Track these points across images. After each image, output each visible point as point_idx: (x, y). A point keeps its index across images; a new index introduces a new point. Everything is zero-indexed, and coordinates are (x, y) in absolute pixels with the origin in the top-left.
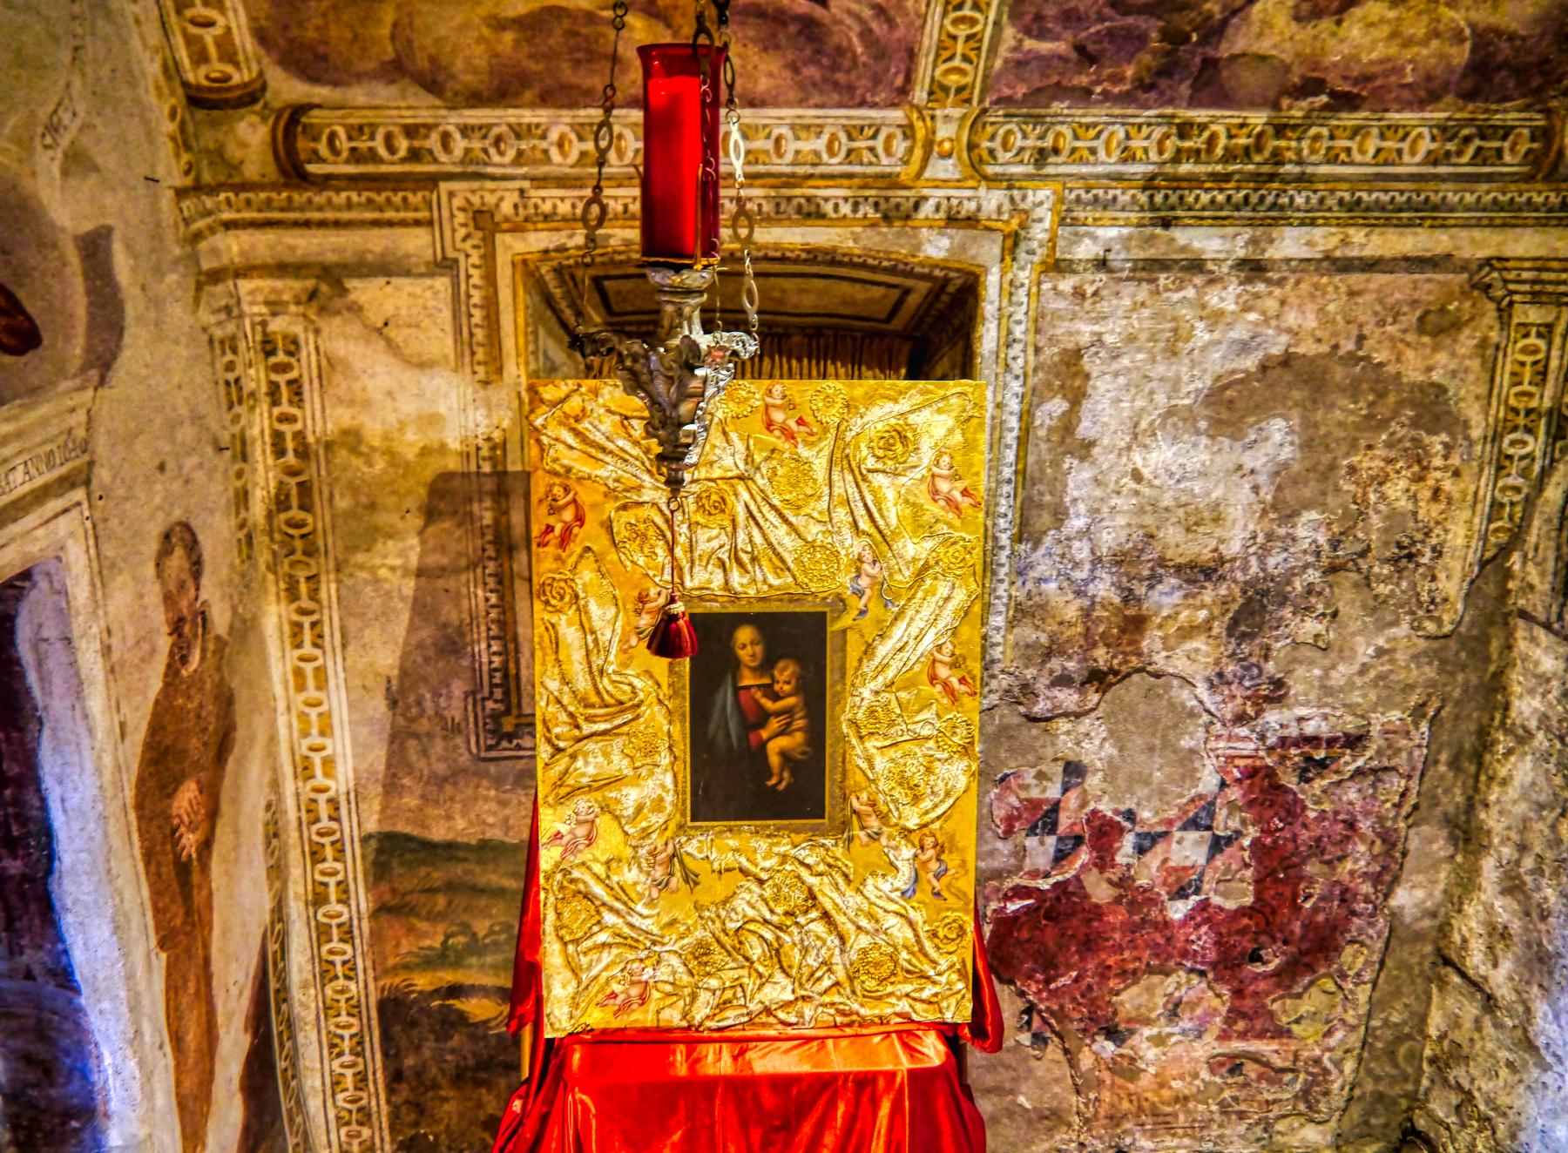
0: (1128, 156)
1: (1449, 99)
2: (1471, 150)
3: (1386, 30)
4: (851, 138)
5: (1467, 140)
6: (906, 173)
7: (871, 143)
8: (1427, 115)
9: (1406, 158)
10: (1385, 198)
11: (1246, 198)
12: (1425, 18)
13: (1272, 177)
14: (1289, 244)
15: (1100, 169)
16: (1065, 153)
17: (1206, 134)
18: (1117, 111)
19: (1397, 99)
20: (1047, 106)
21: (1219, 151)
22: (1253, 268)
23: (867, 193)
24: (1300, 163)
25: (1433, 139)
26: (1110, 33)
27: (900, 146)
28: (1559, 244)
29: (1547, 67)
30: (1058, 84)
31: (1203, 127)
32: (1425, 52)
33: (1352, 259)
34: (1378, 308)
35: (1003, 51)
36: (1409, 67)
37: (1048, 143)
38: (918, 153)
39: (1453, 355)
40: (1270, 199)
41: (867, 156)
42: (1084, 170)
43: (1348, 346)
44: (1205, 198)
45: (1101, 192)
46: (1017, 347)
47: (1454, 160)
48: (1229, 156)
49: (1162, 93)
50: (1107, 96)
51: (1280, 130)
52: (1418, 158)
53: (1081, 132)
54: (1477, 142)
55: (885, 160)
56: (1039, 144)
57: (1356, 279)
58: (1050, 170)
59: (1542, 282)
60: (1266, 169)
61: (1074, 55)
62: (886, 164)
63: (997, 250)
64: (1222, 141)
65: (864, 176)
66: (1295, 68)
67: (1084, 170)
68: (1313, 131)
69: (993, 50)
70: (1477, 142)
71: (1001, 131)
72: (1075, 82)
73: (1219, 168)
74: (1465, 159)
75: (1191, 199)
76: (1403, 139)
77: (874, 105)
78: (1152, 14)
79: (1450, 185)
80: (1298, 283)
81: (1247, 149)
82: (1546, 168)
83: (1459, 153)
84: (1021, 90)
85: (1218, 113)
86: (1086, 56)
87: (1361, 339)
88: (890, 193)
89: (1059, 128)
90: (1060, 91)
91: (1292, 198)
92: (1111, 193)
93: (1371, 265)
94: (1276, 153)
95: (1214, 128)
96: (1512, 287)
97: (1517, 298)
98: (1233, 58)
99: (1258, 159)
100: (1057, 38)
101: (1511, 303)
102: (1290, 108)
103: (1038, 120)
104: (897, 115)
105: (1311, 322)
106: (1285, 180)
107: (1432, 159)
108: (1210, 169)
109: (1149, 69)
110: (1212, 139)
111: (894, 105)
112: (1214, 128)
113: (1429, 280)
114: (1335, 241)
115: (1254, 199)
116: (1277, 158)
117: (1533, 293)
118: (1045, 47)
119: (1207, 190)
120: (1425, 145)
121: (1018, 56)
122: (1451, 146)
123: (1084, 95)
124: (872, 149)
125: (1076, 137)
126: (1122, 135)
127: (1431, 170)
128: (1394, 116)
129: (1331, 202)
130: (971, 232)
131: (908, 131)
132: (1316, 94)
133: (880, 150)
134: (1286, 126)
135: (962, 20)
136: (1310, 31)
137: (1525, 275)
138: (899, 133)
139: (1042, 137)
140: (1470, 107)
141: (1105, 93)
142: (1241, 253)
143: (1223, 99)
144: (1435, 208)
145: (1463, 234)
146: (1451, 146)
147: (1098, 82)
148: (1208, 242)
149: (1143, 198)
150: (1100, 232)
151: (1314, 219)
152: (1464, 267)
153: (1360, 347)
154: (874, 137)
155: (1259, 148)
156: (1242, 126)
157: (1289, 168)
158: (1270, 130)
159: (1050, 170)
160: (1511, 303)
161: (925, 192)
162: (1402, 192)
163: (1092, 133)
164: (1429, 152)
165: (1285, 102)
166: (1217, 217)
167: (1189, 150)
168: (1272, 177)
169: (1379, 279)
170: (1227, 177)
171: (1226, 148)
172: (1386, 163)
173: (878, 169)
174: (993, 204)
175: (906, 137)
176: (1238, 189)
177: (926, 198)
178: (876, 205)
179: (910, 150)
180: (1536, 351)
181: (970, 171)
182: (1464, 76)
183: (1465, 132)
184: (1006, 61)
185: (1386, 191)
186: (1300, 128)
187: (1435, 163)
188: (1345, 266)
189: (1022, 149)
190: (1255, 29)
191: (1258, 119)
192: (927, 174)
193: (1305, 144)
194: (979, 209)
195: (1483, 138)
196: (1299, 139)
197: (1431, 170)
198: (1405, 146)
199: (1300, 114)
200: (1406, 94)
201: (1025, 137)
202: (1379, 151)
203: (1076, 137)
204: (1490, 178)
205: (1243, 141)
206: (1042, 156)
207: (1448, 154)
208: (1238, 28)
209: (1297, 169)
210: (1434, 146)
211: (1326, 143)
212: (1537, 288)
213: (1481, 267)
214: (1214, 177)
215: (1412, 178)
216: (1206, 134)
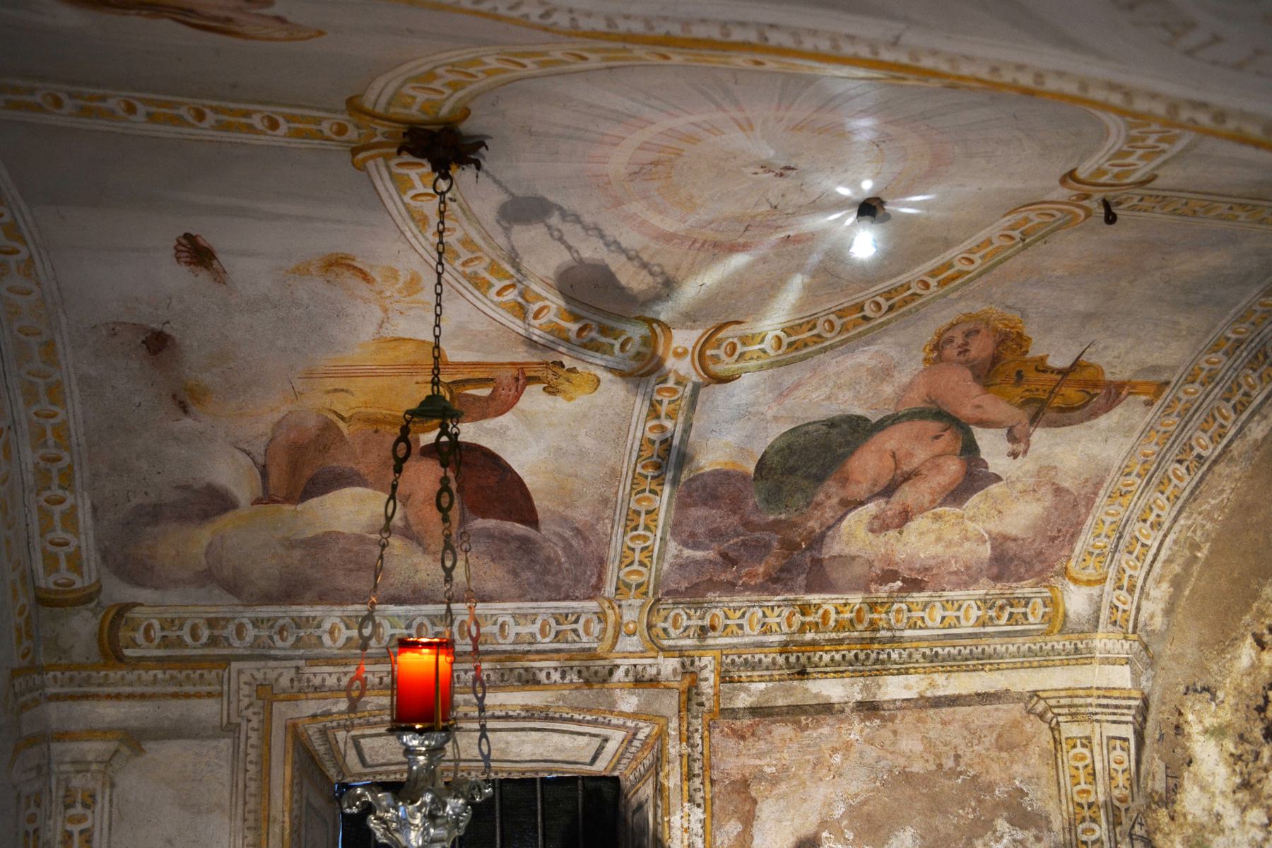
0: (766, 629)
1: (984, 580)
3: (933, 537)
12: (957, 529)
14: (894, 688)
19: (948, 583)
22: (869, 708)
26: (744, 544)
28: (1080, 678)
29: (1042, 558)
32: (961, 550)
33: (940, 697)
34: (966, 733)
35: (669, 558)
39: (1026, 765)
43: (949, 763)
46: (697, 781)
49: (786, 585)
57: (945, 712)
59: (1076, 706)
63: (675, 702)
66: (876, 563)
69: (661, 557)
75: (816, 659)
78: (773, 531)
80: (904, 717)
82: (1058, 626)
86: (728, 560)
87: (957, 757)
93: (953, 701)
96: (1056, 711)
97: (1060, 719)
101: (1058, 723)
105: (919, 748)
109: (774, 567)
113: (996, 710)
114: (924, 684)
117: (1072, 715)
121: (679, 561)
129: (917, 656)
130: (652, 691)
135: (638, 537)
136: (882, 538)
137: (1063, 702)
142: (859, 697)
144: (990, 657)
145: (1014, 673)
148: (833, 689)
149: (781, 660)
150: (753, 686)
151: (907, 669)
152: (1019, 698)
153: (958, 764)
160: (1058, 723)
165: (873, 587)
166: (837, 670)
169: (962, 711)
174: (670, 669)
180: (1083, 758)
181: (650, 645)
182: (990, 566)
184: (671, 565)
186: (886, 605)
188: (938, 702)
190: (845, 538)
194: (659, 673)
200: (954, 578)
204: (1023, 633)
208: (833, 538)
211: (906, 614)
212: (1073, 710)
213: (1031, 698)
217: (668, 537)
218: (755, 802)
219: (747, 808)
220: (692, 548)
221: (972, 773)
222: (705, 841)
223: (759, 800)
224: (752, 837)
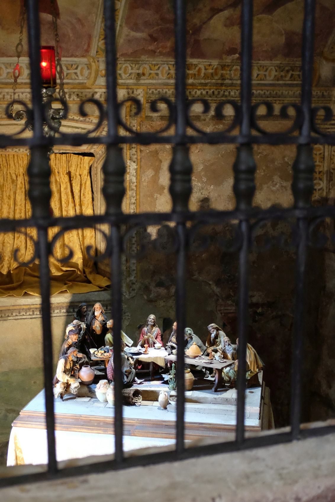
2: (290, 75)
4: (68, 69)
5: (288, 71)
6: (88, 83)
7: (76, 71)
8: (273, 62)
9: (268, 78)
10: (262, 93)
11: (213, 92)
13: (222, 85)
15: (160, 81)
16: (147, 75)
17: (197, 68)
18: (165, 59)
20: (140, 57)
21: (202, 75)
23: (74, 90)
24: (231, 80)
25: (276, 71)
27: (86, 72)
30: (143, 49)
31: (196, 65)
36: (265, 45)
37: (140, 71)
38: (93, 75)
40: (222, 93)
41: (74, 76)
42: (154, 82)
44: (199, 92)
45: (161, 90)
47: (284, 79)
48: (206, 77)
50: (161, 54)
51: (223, 67)
52: (272, 78)
53: (152, 67)
54: (291, 72)
55: (80, 78)
56: (137, 71)
58: (142, 82)
60: (220, 81)
61: (149, 38)
62: (81, 79)
64: (203, 71)
65: (72, 84)
67: (154, 82)
68: (235, 67)
70: (291, 72)
71: (124, 66)
72: (150, 48)
73: (203, 81)
74: (288, 78)
76: (266, 71)
77: (76, 56)
79: (284, 88)
81: (212, 74)
83: (286, 76)
84: (130, 51)
85: (201, 60)
88: (83, 90)
89: (144, 65)
90: (145, 52)
91: (229, 92)
92: (164, 90)
94: (222, 75)
95: (200, 66)
98: (205, 40)
99: (216, 78)
100: (143, 32)
102: (226, 59)
103: (137, 63)
104: (84, 60)
106: (227, 85)
107: (277, 78)
108: (199, 82)
110: (200, 70)
111: (83, 56)
112: (200, 66)
115: (216, 93)
116: (223, 78)
118: (139, 35)
119: (199, 89)
120: (274, 73)
122: (283, 74)
123: (153, 53)
124: (76, 73)
125: (151, 69)
126: (167, 68)
127: (277, 82)
128: (261, 62)
131: (89, 66)
132: (235, 54)
133: (79, 74)
134: (225, 65)
138: (86, 67)
139: (138, 69)
140: (287, 59)
141: (159, 52)
143: (202, 55)
146: (283, 74)
147: (158, 48)
154: (76, 68)
155: (216, 74)
156: (210, 65)
157: (228, 81)
158: (220, 67)
159: (142, 82)
161: (97, 90)
162: (267, 91)
163: (157, 67)
164: (275, 76)
167: (191, 74)
168: (222, 85)
170: (206, 85)
171: (205, 74)
172: (261, 80)
173: (77, 81)
175: (88, 68)
176: (210, 89)
177: (96, 93)
178: (78, 95)
179: (90, 74)
183: (287, 68)
185: (262, 90)
187: (278, 80)
189: (131, 74)
191: (215, 63)
192: (97, 83)
193: (232, 72)
195: (293, 71)
196: (230, 71)
197: (277, 82)
198: (267, 73)
199: (230, 61)
201: (132, 69)
202: (258, 75)
203: (151, 69)
205: (210, 71)
206: (139, 76)
207: (282, 76)
209: (230, 82)
210: (276, 73)
214: (201, 84)
215: (271, 85)
216: (197, 68)
217: (124, 25)
218: (161, 161)
219: (157, 164)
220: (135, 31)
221: (265, 153)
222: (137, 179)
223: (163, 160)
224: (159, 179)
